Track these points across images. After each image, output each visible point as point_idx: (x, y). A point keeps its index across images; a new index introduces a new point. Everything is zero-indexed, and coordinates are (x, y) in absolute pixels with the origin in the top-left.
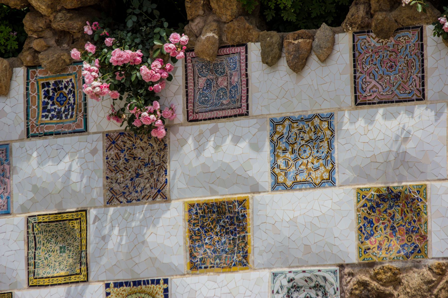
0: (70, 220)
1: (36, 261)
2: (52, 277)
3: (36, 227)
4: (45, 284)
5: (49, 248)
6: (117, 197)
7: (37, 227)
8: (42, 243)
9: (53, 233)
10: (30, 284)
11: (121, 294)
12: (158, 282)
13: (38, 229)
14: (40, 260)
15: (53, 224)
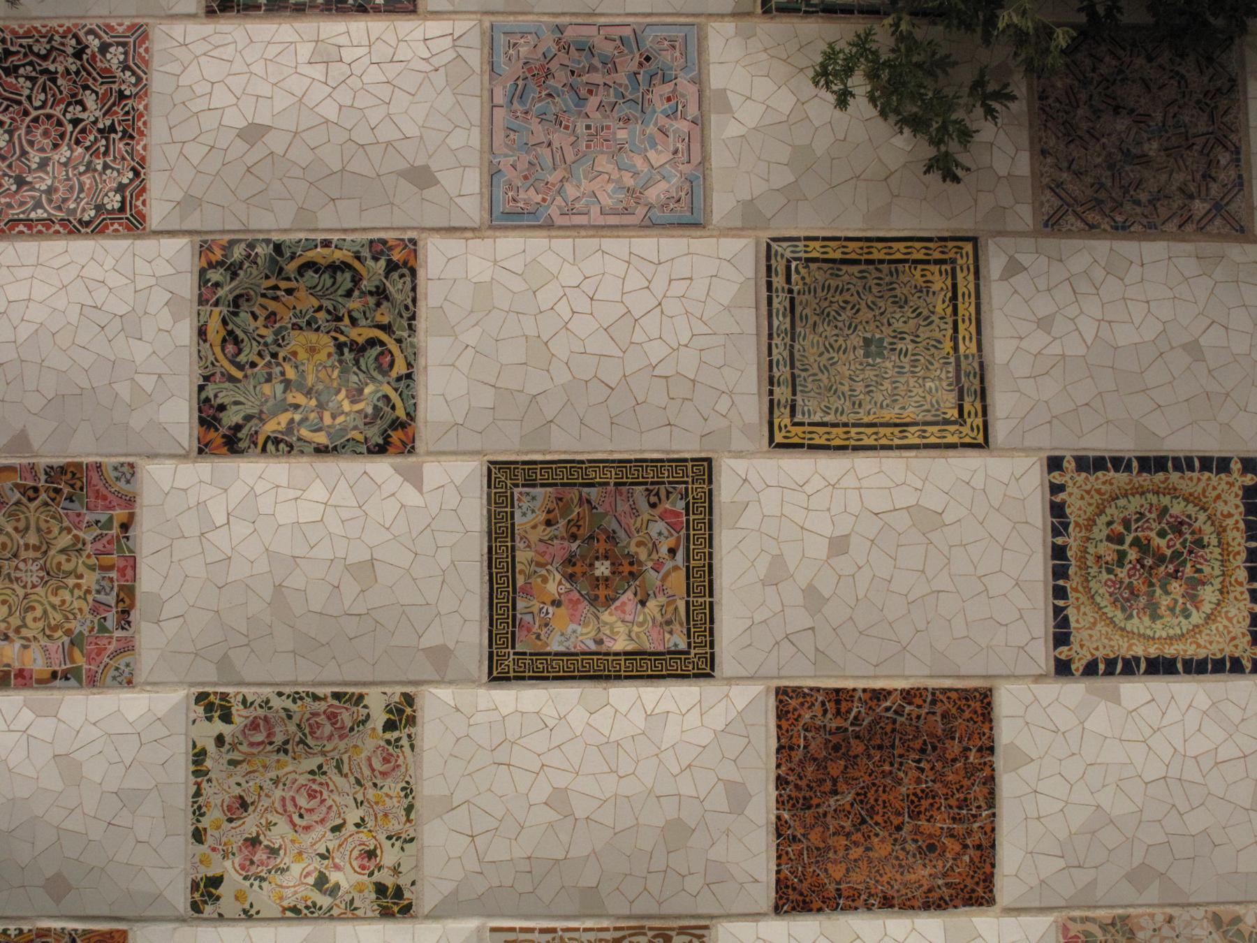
0: (916, 262)
1: (796, 371)
2: (854, 425)
3: (797, 272)
4: (833, 443)
5: (832, 340)
6: (1079, 209)
7: (803, 271)
8: (811, 322)
9: (847, 296)
10: (779, 438)
11: (1098, 491)
12: (1223, 465)
13: (803, 278)
14: (806, 370)
15: (854, 269)
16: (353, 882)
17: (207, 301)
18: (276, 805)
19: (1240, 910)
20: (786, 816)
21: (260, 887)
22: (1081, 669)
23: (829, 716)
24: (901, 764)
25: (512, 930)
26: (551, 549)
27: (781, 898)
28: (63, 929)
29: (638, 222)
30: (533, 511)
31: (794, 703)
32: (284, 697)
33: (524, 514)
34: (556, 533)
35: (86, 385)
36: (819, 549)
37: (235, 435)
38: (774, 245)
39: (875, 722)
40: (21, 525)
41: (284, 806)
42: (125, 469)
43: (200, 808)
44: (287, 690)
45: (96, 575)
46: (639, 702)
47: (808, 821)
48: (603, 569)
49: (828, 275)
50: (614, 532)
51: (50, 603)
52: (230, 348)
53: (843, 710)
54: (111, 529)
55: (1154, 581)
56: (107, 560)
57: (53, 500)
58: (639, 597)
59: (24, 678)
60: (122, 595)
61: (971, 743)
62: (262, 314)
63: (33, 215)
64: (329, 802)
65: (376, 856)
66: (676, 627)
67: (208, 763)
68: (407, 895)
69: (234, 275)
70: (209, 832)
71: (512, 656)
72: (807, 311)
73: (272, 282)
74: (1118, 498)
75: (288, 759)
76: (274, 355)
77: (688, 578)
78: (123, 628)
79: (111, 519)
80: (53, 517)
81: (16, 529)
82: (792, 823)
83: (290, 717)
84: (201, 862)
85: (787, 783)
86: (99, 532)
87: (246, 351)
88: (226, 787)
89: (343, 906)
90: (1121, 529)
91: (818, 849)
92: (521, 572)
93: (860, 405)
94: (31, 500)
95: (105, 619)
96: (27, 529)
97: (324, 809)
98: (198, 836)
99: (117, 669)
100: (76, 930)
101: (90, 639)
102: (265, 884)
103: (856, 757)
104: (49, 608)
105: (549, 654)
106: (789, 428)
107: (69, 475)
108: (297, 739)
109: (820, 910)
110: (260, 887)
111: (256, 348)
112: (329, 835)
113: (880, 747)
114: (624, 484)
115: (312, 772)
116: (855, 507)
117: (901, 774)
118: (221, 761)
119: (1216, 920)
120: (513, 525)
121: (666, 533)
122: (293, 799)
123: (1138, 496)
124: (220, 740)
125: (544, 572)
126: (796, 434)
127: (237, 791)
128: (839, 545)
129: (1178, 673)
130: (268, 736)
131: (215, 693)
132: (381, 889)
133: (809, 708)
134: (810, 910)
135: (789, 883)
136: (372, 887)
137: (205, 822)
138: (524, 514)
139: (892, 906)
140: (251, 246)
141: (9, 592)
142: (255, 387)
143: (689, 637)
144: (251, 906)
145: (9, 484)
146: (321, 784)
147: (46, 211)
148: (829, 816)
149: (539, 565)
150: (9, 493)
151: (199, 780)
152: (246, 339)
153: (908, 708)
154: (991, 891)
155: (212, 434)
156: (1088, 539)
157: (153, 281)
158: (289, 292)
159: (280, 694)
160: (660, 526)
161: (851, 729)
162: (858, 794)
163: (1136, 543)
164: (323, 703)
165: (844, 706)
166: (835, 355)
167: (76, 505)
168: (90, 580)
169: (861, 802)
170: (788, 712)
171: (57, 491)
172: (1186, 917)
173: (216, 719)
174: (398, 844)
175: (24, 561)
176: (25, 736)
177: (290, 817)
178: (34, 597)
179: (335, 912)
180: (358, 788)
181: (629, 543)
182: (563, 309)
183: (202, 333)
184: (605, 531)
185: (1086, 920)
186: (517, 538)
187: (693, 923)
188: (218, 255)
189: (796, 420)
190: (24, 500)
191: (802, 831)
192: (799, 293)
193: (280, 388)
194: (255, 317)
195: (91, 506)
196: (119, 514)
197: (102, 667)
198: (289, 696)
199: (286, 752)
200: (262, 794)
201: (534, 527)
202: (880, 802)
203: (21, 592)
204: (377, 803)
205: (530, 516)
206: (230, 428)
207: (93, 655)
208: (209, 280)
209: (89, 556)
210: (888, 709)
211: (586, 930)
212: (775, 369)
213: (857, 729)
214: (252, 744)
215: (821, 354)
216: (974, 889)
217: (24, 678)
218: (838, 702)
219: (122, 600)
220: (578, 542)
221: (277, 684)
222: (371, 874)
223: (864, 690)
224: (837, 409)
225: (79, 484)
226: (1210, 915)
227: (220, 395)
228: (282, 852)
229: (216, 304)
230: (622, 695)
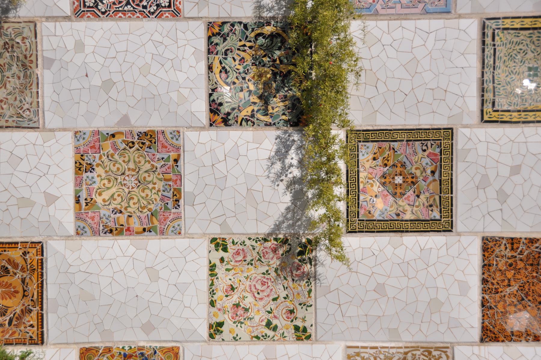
1: (495, 85)
2: (524, 111)
3: (498, 35)
4: (514, 120)
5: (512, 69)
8: (503, 60)
9: (521, 46)
10: (486, 118)
13: (501, 38)
14: (499, 84)
16: (283, 325)
17: (212, 52)
18: (247, 288)
20: (487, 297)
21: (241, 327)
23: (508, 250)
25: (358, 347)
26: (375, 171)
27: (484, 335)
28: (150, 346)
29: (419, 12)
30: (367, 154)
31: (491, 244)
32: (251, 240)
33: (363, 155)
34: (378, 163)
35: (156, 93)
36: (505, 171)
37: (227, 117)
38: (487, 22)
40: (126, 159)
41: (250, 289)
42: (176, 133)
43: (213, 291)
45: (163, 183)
46: (417, 243)
47: (497, 299)
48: (399, 180)
49: (513, 36)
50: (405, 163)
51: (140, 195)
52: (224, 75)
53: (515, 247)
54: (169, 162)
56: (167, 176)
57: (141, 148)
58: (416, 193)
59: (130, 231)
60: (175, 193)
62: (238, 58)
63: (126, 8)
64: (271, 288)
65: (294, 313)
66: (434, 208)
67: (217, 270)
68: (309, 331)
69: (225, 40)
70: (217, 302)
71: (357, 222)
72: (502, 55)
73: (243, 43)
75: (252, 267)
76: (244, 79)
77: (441, 185)
78: (176, 208)
79: (169, 157)
80: (141, 156)
81: (124, 161)
82: (490, 300)
83: (254, 249)
84: (214, 315)
85: (488, 282)
86: (163, 163)
87: (231, 76)
88: (224, 281)
89: (279, 335)
92: (362, 182)
93: (526, 101)
94: (130, 148)
95: (167, 203)
96: (129, 161)
97: (269, 290)
98: (212, 304)
99: (174, 227)
100: (156, 347)
101: (160, 213)
102: (243, 325)
103: (519, 269)
104: (140, 198)
105: (375, 220)
106: (492, 113)
107: (149, 136)
108: (257, 259)
109: (503, 341)
110: (241, 327)
111: (235, 75)
112: (272, 302)
113: (532, 265)
114: (411, 141)
115: (263, 274)
116: (523, 151)
118: (222, 269)
120: (358, 160)
121: (430, 164)
122: (255, 286)
124: (222, 260)
125: (372, 182)
126: (495, 116)
127: (230, 283)
130: (244, 257)
131: (220, 238)
132: (297, 328)
133: (499, 246)
134: (498, 341)
135: (488, 328)
136: (293, 327)
137: (215, 297)
138: (363, 155)
140: (233, 25)
141: (121, 190)
142: (235, 94)
143: (441, 212)
144: (237, 335)
145: (120, 140)
146: (268, 279)
147: (132, 6)
149: (369, 178)
150: (120, 144)
151: (213, 278)
152: (231, 71)
155: (216, 117)
157: (186, 42)
159: (250, 239)
160: (428, 160)
161: (518, 256)
164: (269, 243)
165: (515, 246)
166: (513, 76)
167: (152, 151)
168: (160, 185)
169: (522, 290)
170: (488, 248)
171: (143, 144)
173: (220, 250)
174: (305, 307)
175: (128, 176)
176: (132, 259)
177: (253, 294)
178: (133, 193)
179: (276, 338)
180: (285, 281)
181: (411, 168)
182: (383, 55)
183: (210, 68)
184: (400, 162)
186: (360, 166)
187: (442, 345)
188: (217, 30)
189: (494, 109)
190: (128, 148)
192: (498, 46)
193: (247, 94)
194: (234, 59)
195: (159, 150)
196: (173, 155)
197: (166, 226)
198: (254, 240)
199: (252, 264)
200: (241, 283)
201: (368, 161)
202: (531, 290)
203: (127, 190)
204: (294, 288)
205: (366, 156)
206: (225, 114)
207: (162, 221)
208: (213, 42)
209: (159, 174)
210: (537, 248)
211: (392, 348)
212: (485, 84)
213: (521, 256)
214: (236, 261)
215: (507, 76)
217: (130, 231)
218: (512, 244)
219: (175, 195)
220: (387, 168)
221: (248, 234)
222: (292, 321)
223: (526, 239)
224: (515, 103)
225: (153, 141)
227: (220, 98)
228: (250, 310)
229: (217, 54)
230: (409, 239)
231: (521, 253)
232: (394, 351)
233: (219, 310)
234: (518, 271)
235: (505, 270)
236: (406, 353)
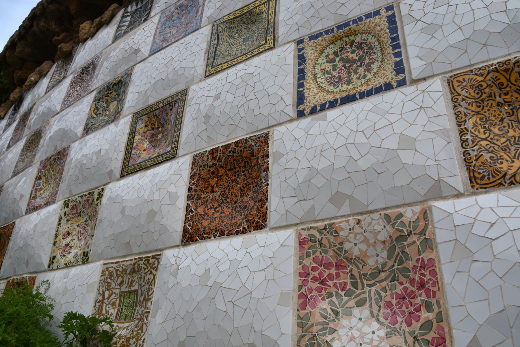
12: (377, 13)
15: (239, 19)
19: (402, 210)
22: (309, 112)
24: (238, 175)
25: (108, 263)
39: (226, 159)
44: (80, 195)
52: (96, 111)
55: (351, 71)
61: (259, 155)
73: (106, 93)
74: (330, 45)
90: (333, 56)
91: (200, 215)
92: (136, 142)
98: (54, 244)
103: (221, 176)
113: (230, 170)
117: (238, 179)
119: (387, 218)
123: (339, 41)
128: (217, 97)
129: (358, 99)
139: (224, 235)
148: (209, 202)
149: (142, 140)
153: (237, 148)
154: (266, 221)
156: (316, 64)
158: (111, 93)
162: (222, 191)
163: (341, 60)
169: (223, 194)
172: (368, 219)
185: (309, 229)
191: (195, 208)
194: (103, 102)
199: (81, 216)
201: (142, 128)
205: (141, 125)
210: (230, 152)
213: (220, 163)
214: (73, 214)
216: (258, 222)
223: (222, 146)
226: (383, 216)
231: (219, 160)
232: (128, 263)
233: (57, 247)
234: (220, 178)
235: (208, 178)
236: (135, 264)
